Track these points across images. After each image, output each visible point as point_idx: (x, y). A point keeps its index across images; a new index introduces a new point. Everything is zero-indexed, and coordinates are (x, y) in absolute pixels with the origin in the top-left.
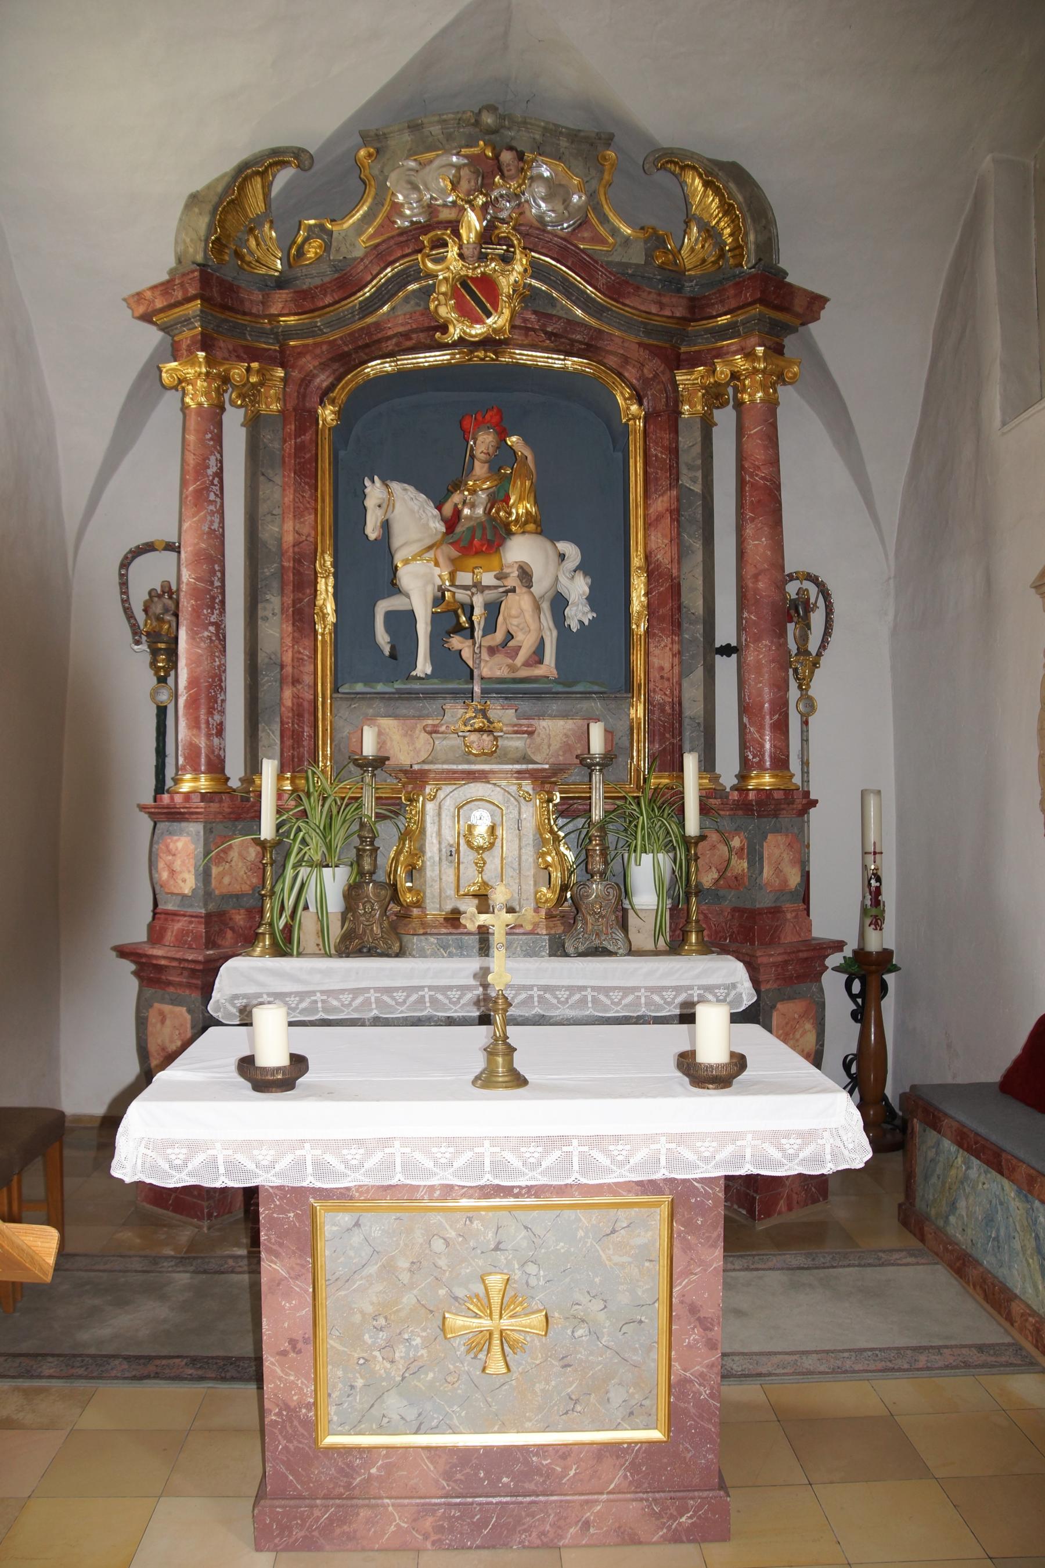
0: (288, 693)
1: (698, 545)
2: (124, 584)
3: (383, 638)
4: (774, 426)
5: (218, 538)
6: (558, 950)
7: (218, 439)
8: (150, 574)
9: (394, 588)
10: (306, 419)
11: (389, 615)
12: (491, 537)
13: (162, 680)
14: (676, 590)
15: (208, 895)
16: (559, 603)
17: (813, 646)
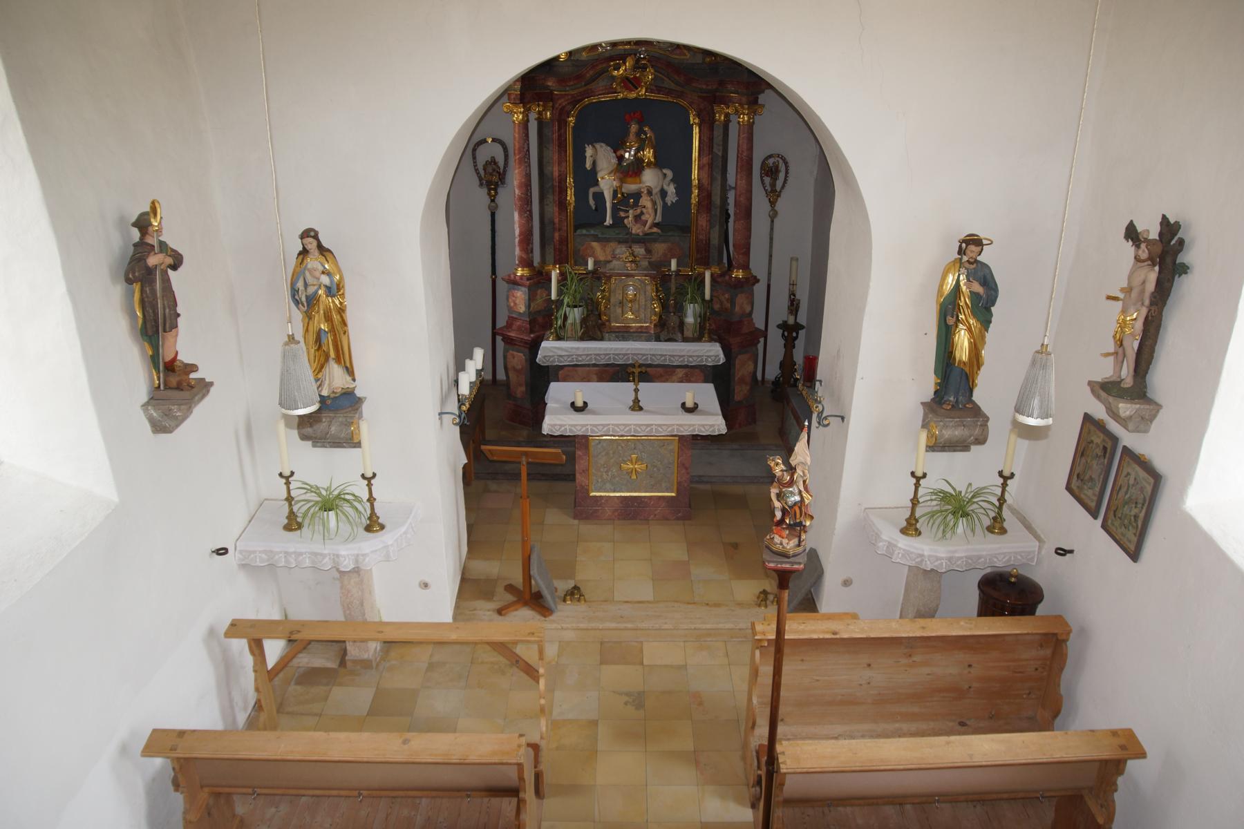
0: (557, 235)
1: (719, 178)
2: (474, 158)
3: (592, 202)
4: (751, 134)
5: (528, 176)
6: (658, 339)
7: (527, 135)
8: (484, 155)
9: (596, 183)
10: (563, 123)
11: (594, 194)
12: (636, 168)
13: (493, 201)
14: (709, 196)
15: (530, 313)
16: (663, 193)
17: (778, 188)
